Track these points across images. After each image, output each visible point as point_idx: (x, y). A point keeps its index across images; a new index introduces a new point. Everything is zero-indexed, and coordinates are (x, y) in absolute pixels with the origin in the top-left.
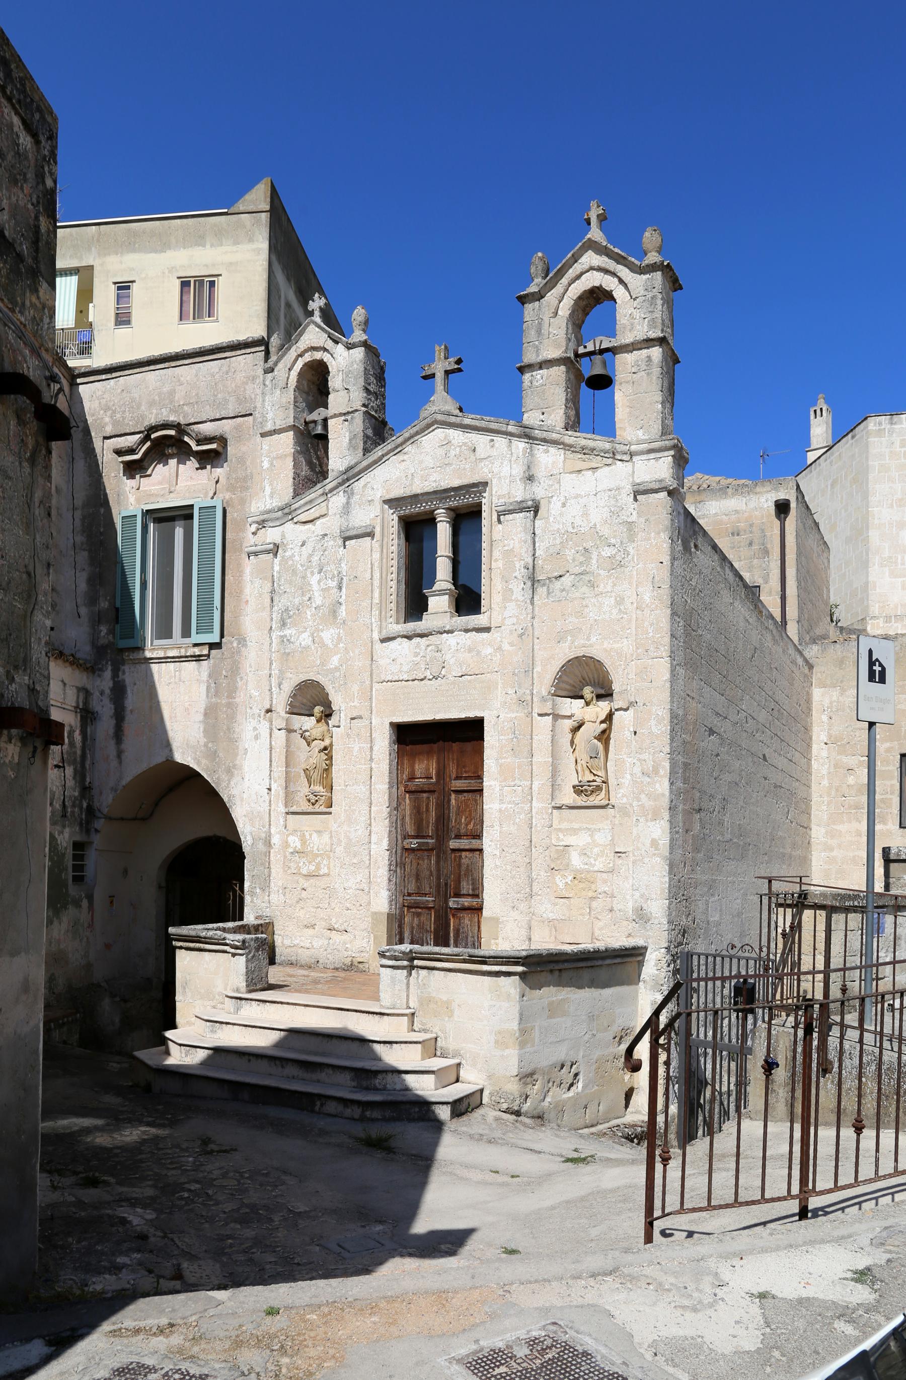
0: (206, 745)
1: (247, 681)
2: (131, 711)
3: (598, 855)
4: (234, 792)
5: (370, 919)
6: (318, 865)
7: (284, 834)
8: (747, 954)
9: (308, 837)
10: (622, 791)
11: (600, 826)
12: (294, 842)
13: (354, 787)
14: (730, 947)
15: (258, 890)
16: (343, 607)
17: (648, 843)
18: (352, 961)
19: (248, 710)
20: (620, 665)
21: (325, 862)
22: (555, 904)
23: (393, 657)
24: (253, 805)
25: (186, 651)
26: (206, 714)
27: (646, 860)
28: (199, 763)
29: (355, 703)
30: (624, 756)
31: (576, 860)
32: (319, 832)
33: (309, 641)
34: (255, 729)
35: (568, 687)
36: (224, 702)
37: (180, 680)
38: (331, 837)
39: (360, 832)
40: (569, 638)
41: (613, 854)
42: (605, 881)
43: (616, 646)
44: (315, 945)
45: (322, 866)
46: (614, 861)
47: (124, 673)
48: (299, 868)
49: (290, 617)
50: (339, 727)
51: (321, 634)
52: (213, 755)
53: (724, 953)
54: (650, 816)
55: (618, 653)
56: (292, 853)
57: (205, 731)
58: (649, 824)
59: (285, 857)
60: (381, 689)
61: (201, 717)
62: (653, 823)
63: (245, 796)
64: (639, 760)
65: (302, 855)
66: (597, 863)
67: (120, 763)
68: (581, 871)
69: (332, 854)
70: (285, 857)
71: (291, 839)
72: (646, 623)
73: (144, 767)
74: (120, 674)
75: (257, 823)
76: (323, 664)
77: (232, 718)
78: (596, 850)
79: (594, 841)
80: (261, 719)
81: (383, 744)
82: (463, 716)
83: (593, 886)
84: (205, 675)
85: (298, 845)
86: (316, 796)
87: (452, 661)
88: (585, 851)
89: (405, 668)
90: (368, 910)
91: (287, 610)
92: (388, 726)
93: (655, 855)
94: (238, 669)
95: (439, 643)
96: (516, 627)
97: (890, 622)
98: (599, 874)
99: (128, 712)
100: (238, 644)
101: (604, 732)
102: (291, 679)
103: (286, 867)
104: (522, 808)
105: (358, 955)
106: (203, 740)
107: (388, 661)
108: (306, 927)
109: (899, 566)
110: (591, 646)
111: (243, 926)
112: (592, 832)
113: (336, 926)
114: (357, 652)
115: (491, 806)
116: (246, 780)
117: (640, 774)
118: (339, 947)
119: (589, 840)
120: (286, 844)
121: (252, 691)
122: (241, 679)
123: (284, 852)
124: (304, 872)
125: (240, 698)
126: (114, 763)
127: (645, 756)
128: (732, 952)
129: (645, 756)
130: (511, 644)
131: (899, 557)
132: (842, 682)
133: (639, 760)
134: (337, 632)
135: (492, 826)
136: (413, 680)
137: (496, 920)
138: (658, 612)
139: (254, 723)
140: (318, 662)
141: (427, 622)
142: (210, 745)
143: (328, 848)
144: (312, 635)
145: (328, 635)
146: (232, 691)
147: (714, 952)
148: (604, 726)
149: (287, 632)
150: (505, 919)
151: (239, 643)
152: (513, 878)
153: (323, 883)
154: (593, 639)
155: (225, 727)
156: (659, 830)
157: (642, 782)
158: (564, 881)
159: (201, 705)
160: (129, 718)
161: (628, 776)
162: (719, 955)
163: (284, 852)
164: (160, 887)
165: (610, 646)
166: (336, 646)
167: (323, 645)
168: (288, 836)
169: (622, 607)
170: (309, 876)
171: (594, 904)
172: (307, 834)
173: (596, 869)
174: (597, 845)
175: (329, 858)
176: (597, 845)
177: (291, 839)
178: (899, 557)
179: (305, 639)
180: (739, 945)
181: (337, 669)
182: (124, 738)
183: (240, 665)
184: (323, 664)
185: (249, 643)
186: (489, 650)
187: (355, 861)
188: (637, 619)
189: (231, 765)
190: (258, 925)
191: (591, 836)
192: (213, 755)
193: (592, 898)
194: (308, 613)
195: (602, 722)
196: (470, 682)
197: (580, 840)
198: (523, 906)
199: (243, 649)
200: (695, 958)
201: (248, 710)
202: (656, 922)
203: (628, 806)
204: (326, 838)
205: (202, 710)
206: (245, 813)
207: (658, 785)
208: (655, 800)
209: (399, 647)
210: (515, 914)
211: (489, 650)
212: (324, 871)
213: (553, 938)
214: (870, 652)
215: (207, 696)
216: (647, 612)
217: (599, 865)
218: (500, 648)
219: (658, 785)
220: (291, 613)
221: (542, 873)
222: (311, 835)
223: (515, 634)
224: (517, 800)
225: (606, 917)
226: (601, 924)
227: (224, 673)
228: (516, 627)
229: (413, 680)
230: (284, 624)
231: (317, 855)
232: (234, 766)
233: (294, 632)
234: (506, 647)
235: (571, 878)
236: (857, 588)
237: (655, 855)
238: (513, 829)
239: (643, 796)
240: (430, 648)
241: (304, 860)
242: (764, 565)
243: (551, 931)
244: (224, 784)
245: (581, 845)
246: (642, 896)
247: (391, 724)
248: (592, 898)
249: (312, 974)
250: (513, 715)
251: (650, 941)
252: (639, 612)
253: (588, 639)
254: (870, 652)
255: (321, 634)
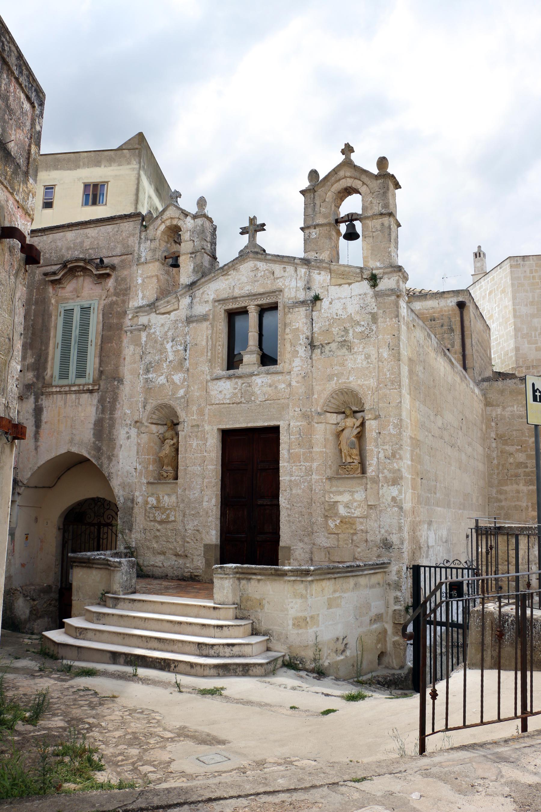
0: (94, 443)
1: (123, 405)
2: (46, 423)
3: (357, 507)
4: (112, 471)
5: (202, 549)
6: (168, 515)
7: (145, 496)
8: (457, 566)
9: (161, 498)
10: (371, 468)
11: (358, 489)
12: (152, 501)
13: (193, 468)
14: (445, 562)
15: (127, 531)
16: (187, 361)
17: (389, 499)
18: (191, 575)
19: (123, 422)
20: (369, 394)
21: (172, 513)
22: (328, 538)
23: (220, 389)
24: (125, 479)
25: (84, 387)
26: (95, 424)
27: (389, 509)
28: (89, 453)
29: (194, 417)
30: (373, 447)
31: (342, 511)
32: (169, 495)
33: (165, 381)
34: (127, 433)
35: (334, 406)
36: (107, 417)
37: (79, 403)
38: (177, 498)
39: (196, 495)
40: (335, 378)
41: (366, 507)
42: (362, 523)
43: (366, 383)
44: (165, 565)
45: (171, 516)
46: (367, 511)
47: (42, 400)
48: (155, 517)
49: (152, 367)
50: (183, 431)
51: (173, 377)
52: (98, 449)
53: (442, 565)
54: (390, 483)
55: (367, 387)
56: (150, 508)
57: (94, 434)
58: (390, 487)
59: (146, 510)
60: (211, 409)
61: (92, 426)
62: (393, 487)
63: (119, 473)
64: (383, 449)
65: (157, 509)
66: (356, 512)
67: (37, 453)
68: (345, 517)
69: (177, 509)
70: (146, 510)
71: (150, 499)
72: (385, 370)
73: (53, 455)
74: (40, 400)
75: (127, 489)
76: (173, 394)
77: (112, 426)
78: (355, 504)
79: (354, 499)
80: (132, 427)
81: (212, 442)
82: (266, 424)
83: (354, 527)
84: (95, 402)
85: (155, 502)
86: (167, 473)
87: (258, 392)
88: (348, 505)
89: (228, 397)
90: (202, 543)
91: (150, 363)
92: (216, 431)
93: (394, 506)
94: (117, 397)
95: (250, 382)
96: (300, 372)
97: (530, 369)
98: (357, 519)
99: (43, 424)
100: (118, 383)
101: (359, 433)
102: (152, 403)
103: (146, 516)
104: (306, 479)
105: (194, 571)
106: (93, 440)
107: (216, 392)
108: (159, 554)
109: (533, 338)
110: (350, 383)
111: (117, 553)
112: (352, 493)
113: (180, 553)
114: (196, 387)
115: (285, 478)
116: (120, 463)
117: (383, 458)
118: (182, 566)
119: (351, 498)
120: (147, 503)
121: (126, 410)
122: (119, 403)
123: (145, 507)
124: (158, 519)
125: (118, 414)
126: (34, 453)
127: (387, 447)
128: (447, 565)
129: (387, 447)
130: (297, 382)
131: (533, 334)
132: (503, 403)
133: (383, 449)
134: (183, 375)
135: (286, 490)
136: (233, 403)
137: (288, 548)
138: (392, 363)
139: (127, 429)
140: (170, 393)
141: (242, 370)
142: (97, 442)
143: (175, 504)
144: (167, 377)
145: (177, 378)
146: (113, 409)
147: (434, 565)
148: (359, 430)
149: (150, 376)
150: (295, 547)
151: (119, 382)
152: (300, 522)
153: (170, 526)
154: (351, 379)
155: (107, 432)
156: (397, 491)
157: (385, 463)
158: (334, 524)
159: (93, 419)
160: (43, 426)
161: (376, 460)
162: (438, 567)
163: (145, 507)
164: (59, 529)
165: (362, 383)
166: (182, 384)
167: (174, 383)
168: (148, 497)
169: (369, 361)
170: (161, 522)
171: (355, 538)
172: (161, 496)
173: (355, 515)
174: (356, 501)
175: (175, 510)
176: (356, 501)
177: (150, 499)
178: (533, 334)
179: (162, 380)
180: (451, 561)
181: (182, 397)
182: (40, 438)
183: (119, 396)
184: (173, 394)
185: (125, 383)
186: (283, 386)
187: (193, 512)
188: (379, 367)
189: (111, 454)
190: (127, 553)
191: (352, 495)
192: (98, 449)
193: (353, 534)
194: (165, 365)
195: (357, 427)
196: (270, 404)
197: (345, 498)
198: (306, 539)
199: (121, 386)
200: (422, 569)
201: (123, 422)
202: (396, 547)
203: (376, 477)
204: (174, 498)
205: (93, 422)
206: (119, 483)
207: (395, 465)
208: (394, 473)
209: (223, 384)
210: (301, 545)
211: (283, 386)
212: (172, 518)
213: (327, 559)
214: (533, 385)
215: (96, 413)
216: (385, 363)
217: (357, 513)
218: (290, 385)
219: (395, 465)
220: (153, 365)
221: (319, 519)
222: (163, 497)
223: (300, 377)
224: (302, 474)
225: (363, 546)
226: (359, 550)
227: (108, 400)
228: (300, 372)
229: (233, 403)
230: (147, 371)
231: (167, 509)
232: (113, 455)
233: (155, 376)
234: (294, 383)
235: (338, 521)
236: (508, 350)
237: (394, 506)
238: (300, 492)
239: (385, 471)
240: (244, 385)
241: (158, 512)
242: (451, 338)
243: (325, 554)
244: (105, 466)
245: (345, 501)
246: (386, 531)
247: (218, 429)
248: (353, 534)
249: (164, 583)
250: (299, 424)
251: (392, 559)
252: (380, 363)
253: (348, 379)
254: (533, 385)
255: (173, 377)
